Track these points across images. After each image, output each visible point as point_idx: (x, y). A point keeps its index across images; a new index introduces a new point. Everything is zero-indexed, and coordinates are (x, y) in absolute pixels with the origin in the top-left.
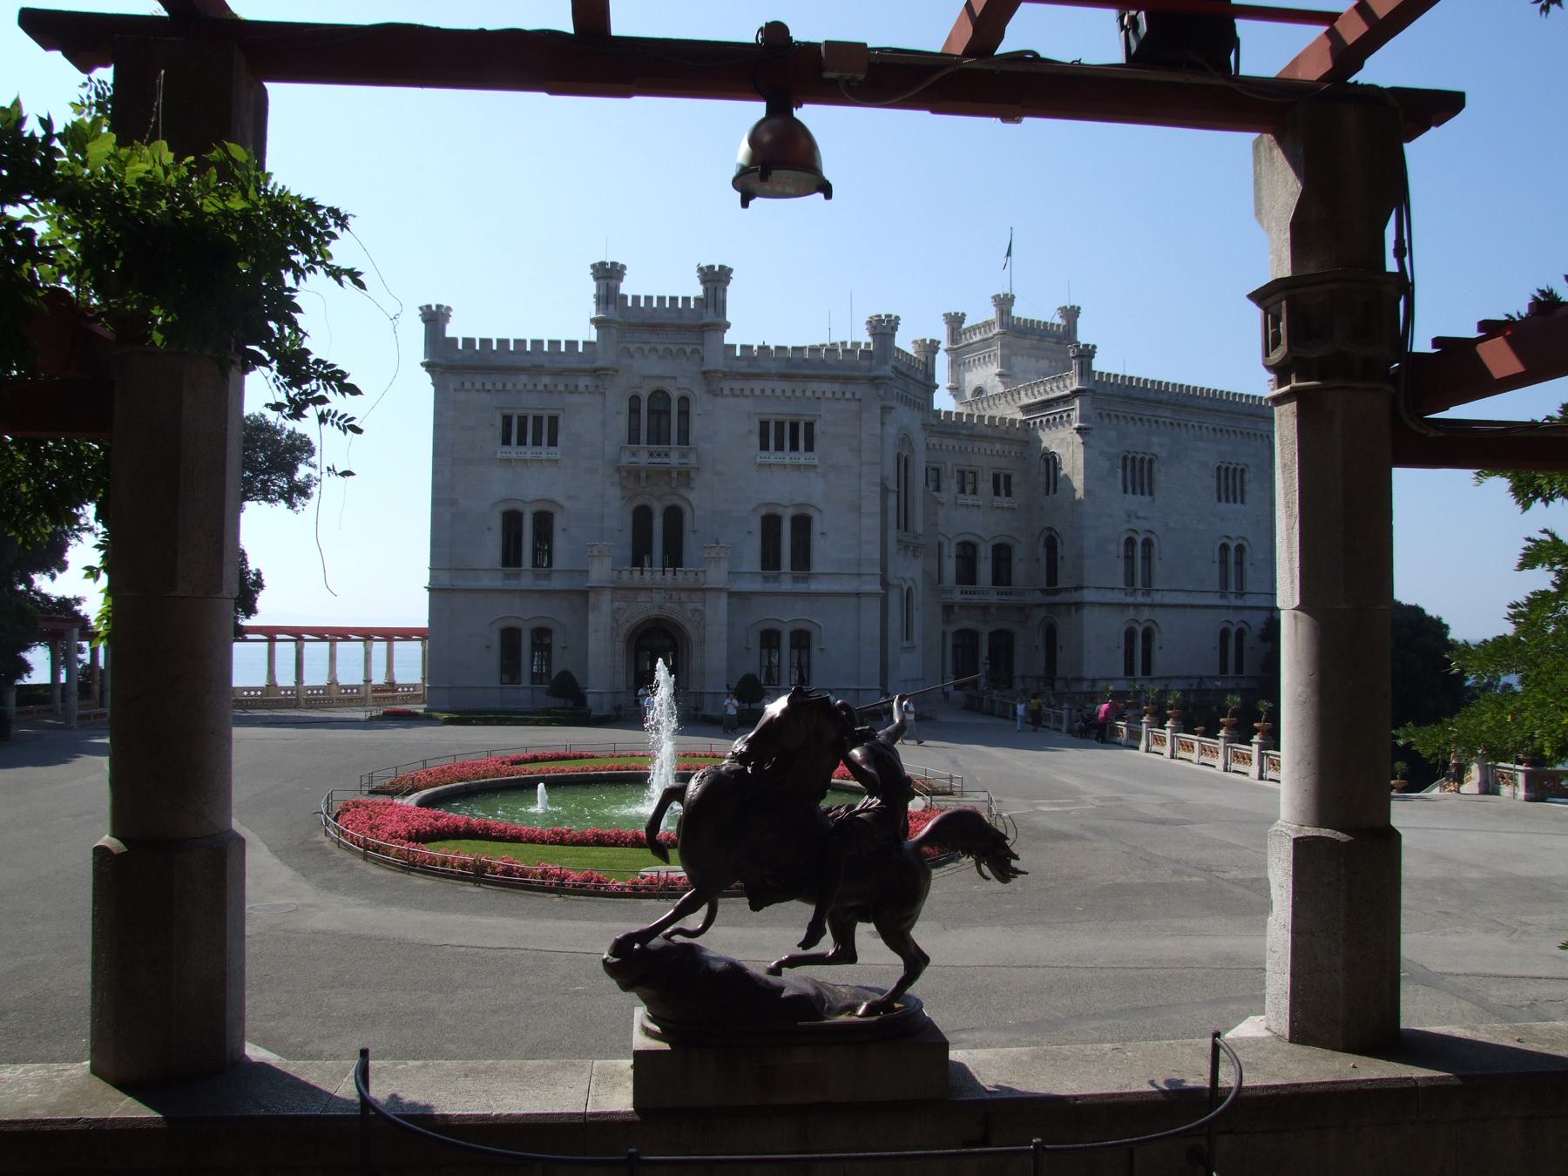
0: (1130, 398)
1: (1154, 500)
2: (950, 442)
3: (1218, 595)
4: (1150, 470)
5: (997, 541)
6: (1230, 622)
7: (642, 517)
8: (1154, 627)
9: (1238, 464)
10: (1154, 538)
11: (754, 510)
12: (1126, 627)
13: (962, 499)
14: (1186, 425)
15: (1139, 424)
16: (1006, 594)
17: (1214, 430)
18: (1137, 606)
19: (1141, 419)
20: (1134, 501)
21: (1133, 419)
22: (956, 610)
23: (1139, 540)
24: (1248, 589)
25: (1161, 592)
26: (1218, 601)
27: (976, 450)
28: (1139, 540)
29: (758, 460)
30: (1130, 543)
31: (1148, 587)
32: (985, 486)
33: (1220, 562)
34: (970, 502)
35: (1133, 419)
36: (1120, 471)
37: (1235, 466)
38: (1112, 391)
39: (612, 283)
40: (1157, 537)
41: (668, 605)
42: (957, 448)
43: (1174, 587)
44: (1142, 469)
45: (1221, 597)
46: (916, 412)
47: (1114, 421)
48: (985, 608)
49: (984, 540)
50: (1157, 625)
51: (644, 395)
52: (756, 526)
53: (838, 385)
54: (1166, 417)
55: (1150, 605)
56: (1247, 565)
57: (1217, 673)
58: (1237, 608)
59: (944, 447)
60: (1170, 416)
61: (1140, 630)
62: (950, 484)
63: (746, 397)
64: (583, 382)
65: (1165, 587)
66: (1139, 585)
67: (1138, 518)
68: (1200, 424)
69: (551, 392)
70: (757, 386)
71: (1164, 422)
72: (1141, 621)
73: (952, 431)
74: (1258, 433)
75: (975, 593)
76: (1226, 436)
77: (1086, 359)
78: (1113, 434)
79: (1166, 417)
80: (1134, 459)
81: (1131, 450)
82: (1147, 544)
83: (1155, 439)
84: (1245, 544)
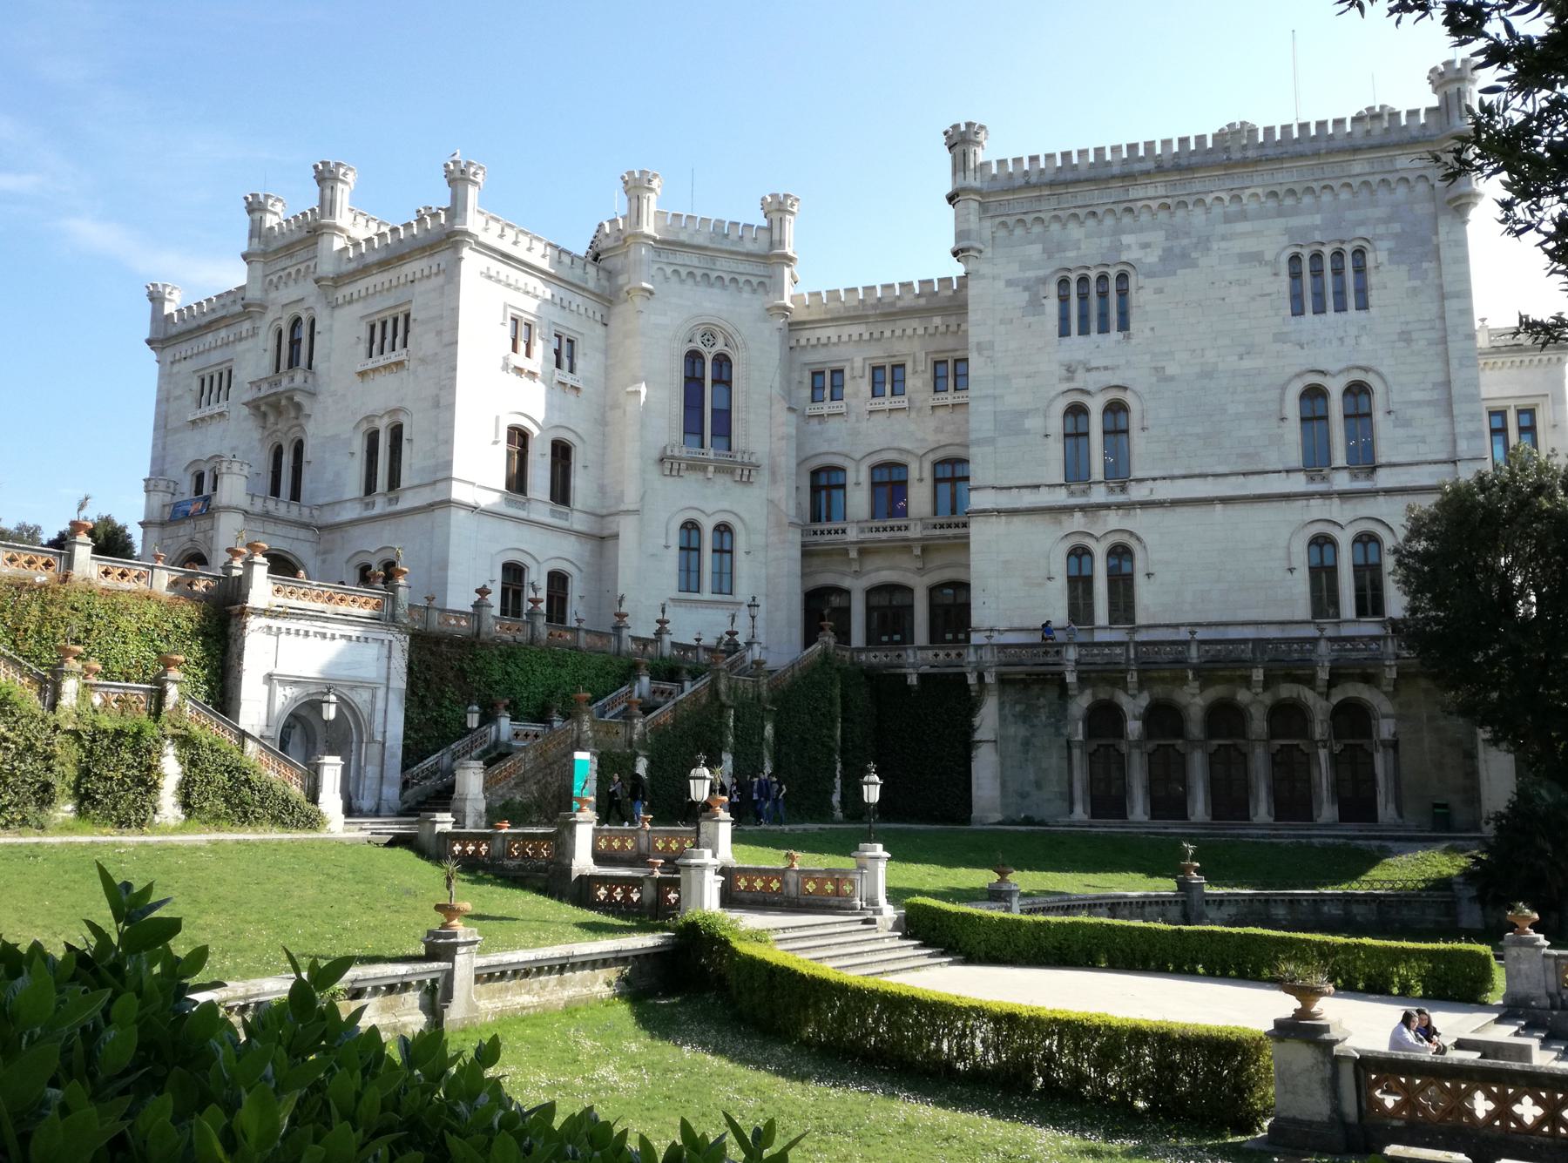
0: (1067, 183)
1: (1128, 337)
2: (855, 330)
3: (1301, 477)
4: (1123, 293)
5: (940, 455)
6: (1335, 523)
7: (278, 454)
8: (1133, 543)
9: (1343, 242)
10: (1129, 398)
11: (356, 427)
12: (1065, 546)
13: (880, 403)
14: (1200, 202)
15: (1091, 222)
16: (942, 526)
17: (1274, 194)
18: (1083, 508)
19: (1094, 214)
20: (1078, 348)
21: (1075, 216)
22: (853, 554)
23: (1096, 406)
24: (1383, 454)
25: (1150, 484)
26: (1298, 483)
27: (898, 332)
28: (1096, 406)
29: (360, 369)
30: (1077, 411)
31: (1118, 475)
32: (917, 382)
33: (1303, 419)
34: (887, 406)
35: (1075, 216)
36: (1052, 306)
37: (1338, 245)
38: (1027, 183)
39: (257, 215)
40: (1135, 392)
41: (197, 536)
42: (866, 336)
43: (1177, 472)
44: (1103, 295)
45: (1311, 479)
46: (746, 295)
47: (1037, 229)
48: (905, 546)
49: (916, 455)
50: (1138, 539)
51: (285, 325)
52: (359, 445)
53: (425, 260)
54: (1149, 199)
55: (1119, 506)
56: (1378, 416)
57: (1303, 610)
58: (1344, 495)
59: (845, 338)
60: (1161, 191)
61: (1100, 551)
62: (858, 388)
63: (357, 300)
64: (246, 326)
65: (1156, 474)
66: (1097, 472)
67: (1088, 370)
68: (1234, 192)
69: (227, 344)
70: (362, 285)
71: (1149, 207)
72: (1096, 534)
73: (859, 313)
74: (1391, 177)
75: (885, 530)
76: (1307, 200)
77: (958, 149)
78: (1035, 250)
79: (1149, 199)
80: (1083, 280)
81: (1071, 266)
82: (1116, 409)
83: (1127, 239)
84: (1371, 379)
